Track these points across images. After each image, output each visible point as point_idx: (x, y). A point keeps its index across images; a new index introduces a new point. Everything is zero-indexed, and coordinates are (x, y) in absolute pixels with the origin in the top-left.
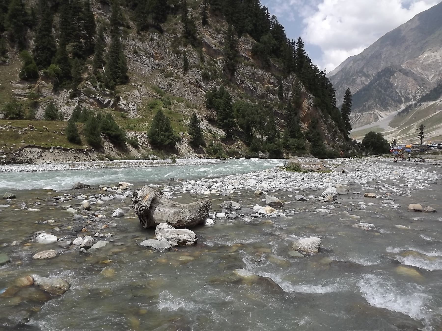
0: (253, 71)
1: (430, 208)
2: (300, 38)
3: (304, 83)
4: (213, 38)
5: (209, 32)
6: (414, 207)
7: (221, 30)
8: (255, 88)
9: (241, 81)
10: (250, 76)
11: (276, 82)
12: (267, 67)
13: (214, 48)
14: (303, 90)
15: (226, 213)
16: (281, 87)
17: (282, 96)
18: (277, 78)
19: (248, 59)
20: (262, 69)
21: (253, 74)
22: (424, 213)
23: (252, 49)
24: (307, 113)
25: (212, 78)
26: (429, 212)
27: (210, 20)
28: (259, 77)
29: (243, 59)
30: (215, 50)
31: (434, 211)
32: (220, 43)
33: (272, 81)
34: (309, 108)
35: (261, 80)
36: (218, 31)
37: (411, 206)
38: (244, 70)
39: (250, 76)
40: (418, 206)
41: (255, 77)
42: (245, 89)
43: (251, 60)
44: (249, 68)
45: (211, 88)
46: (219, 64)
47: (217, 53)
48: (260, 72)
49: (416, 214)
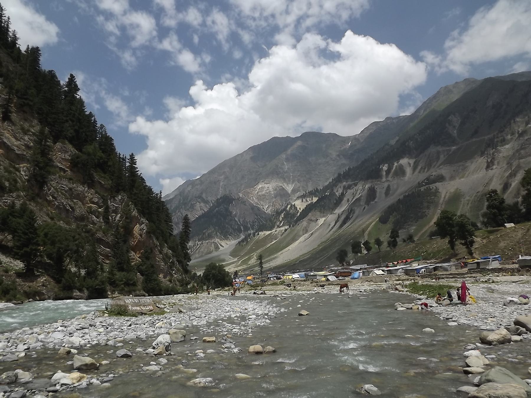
0: (71, 186)
1: (270, 348)
2: (132, 154)
3: (136, 205)
4: (17, 139)
5: (12, 130)
6: (254, 349)
7: (29, 131)
8: (72, 208)
9: (53, 197)
10: (66, 191)
11: (101, 201)
12: (91, 183)
13: (17, 152)
14: (135, 213)
15: (5, 392)
16: (107, 208)
17: (108, 219)
18: (103, 197)
19: (65, 171)
20: (83, 184)
21: (70, 189)
22: (264, 355)
23: (72, 160)
24: (139, 241)
25: (9, 190)
26: (269, 353)
27: (14, 116)
28: (78, 195)
29: (57, 169)
30: (18, 155)
31: (274, 351)
32: (28, 147)
33: (96, 200)
34: (141, 235)
35: (81, 198)
36: (25, 132)
37: (252, 349)
38: (58, 184)
39: (66, 191)
40: (258, 347)
41: (73, 194)
42: (58, 207)
43: (69, 172)
44: (65, 182)
45: (7, 202)
46: (23, 173)
47: (21, 158)
48: (81, 188)
49: (257, 357)
